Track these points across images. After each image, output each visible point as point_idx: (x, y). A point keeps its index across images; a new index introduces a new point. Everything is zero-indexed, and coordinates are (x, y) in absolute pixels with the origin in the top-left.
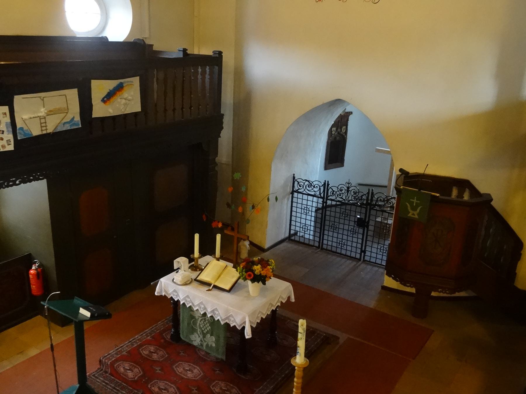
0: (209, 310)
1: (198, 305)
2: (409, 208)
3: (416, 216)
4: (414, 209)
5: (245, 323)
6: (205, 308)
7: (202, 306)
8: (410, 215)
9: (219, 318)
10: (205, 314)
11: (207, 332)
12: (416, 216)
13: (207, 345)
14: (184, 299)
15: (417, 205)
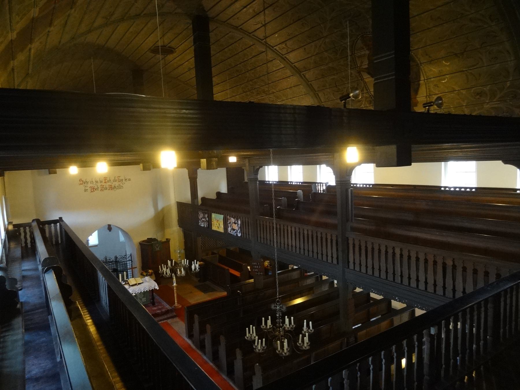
0: (142, 290)
1: (138, 290)
2: (156, 248)
3: (159, 249)
4: (157, 247)
5: (155, 286)
6: (141, 290)
7: (140, 290)
8: (157, 250)
9: (147, 290)
10: (141, 292)
11: (142, 298)
12: (159, 249)
13: (143, 302)
14: (132, 292)
15: (158, 246)
